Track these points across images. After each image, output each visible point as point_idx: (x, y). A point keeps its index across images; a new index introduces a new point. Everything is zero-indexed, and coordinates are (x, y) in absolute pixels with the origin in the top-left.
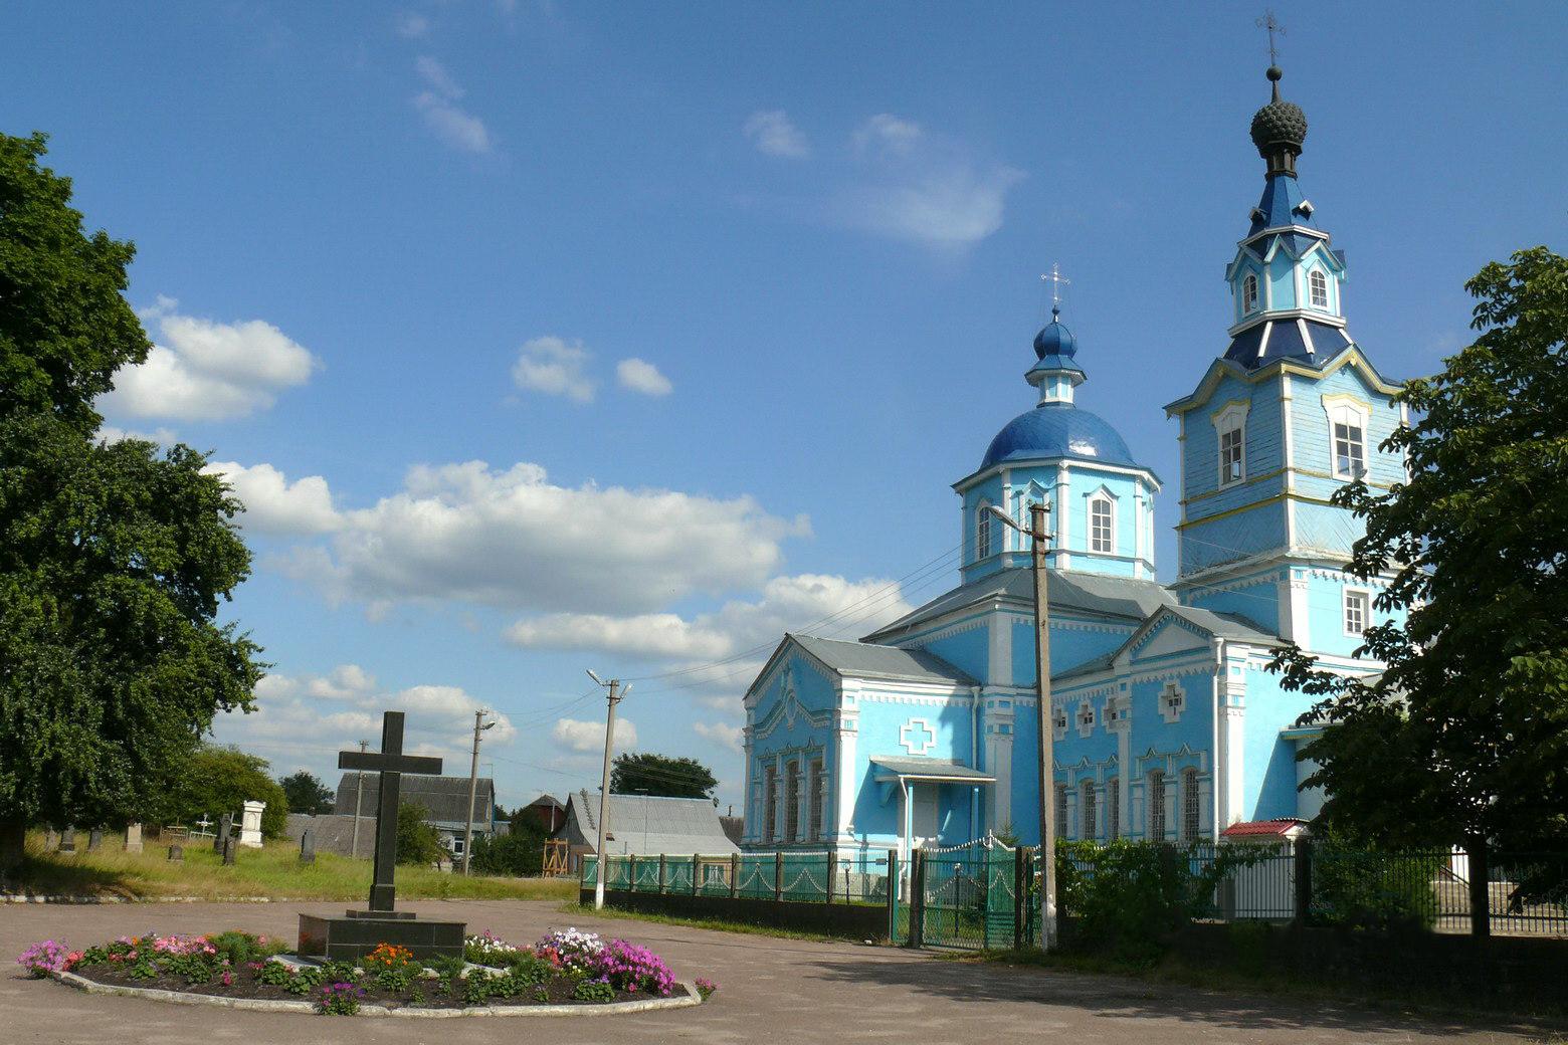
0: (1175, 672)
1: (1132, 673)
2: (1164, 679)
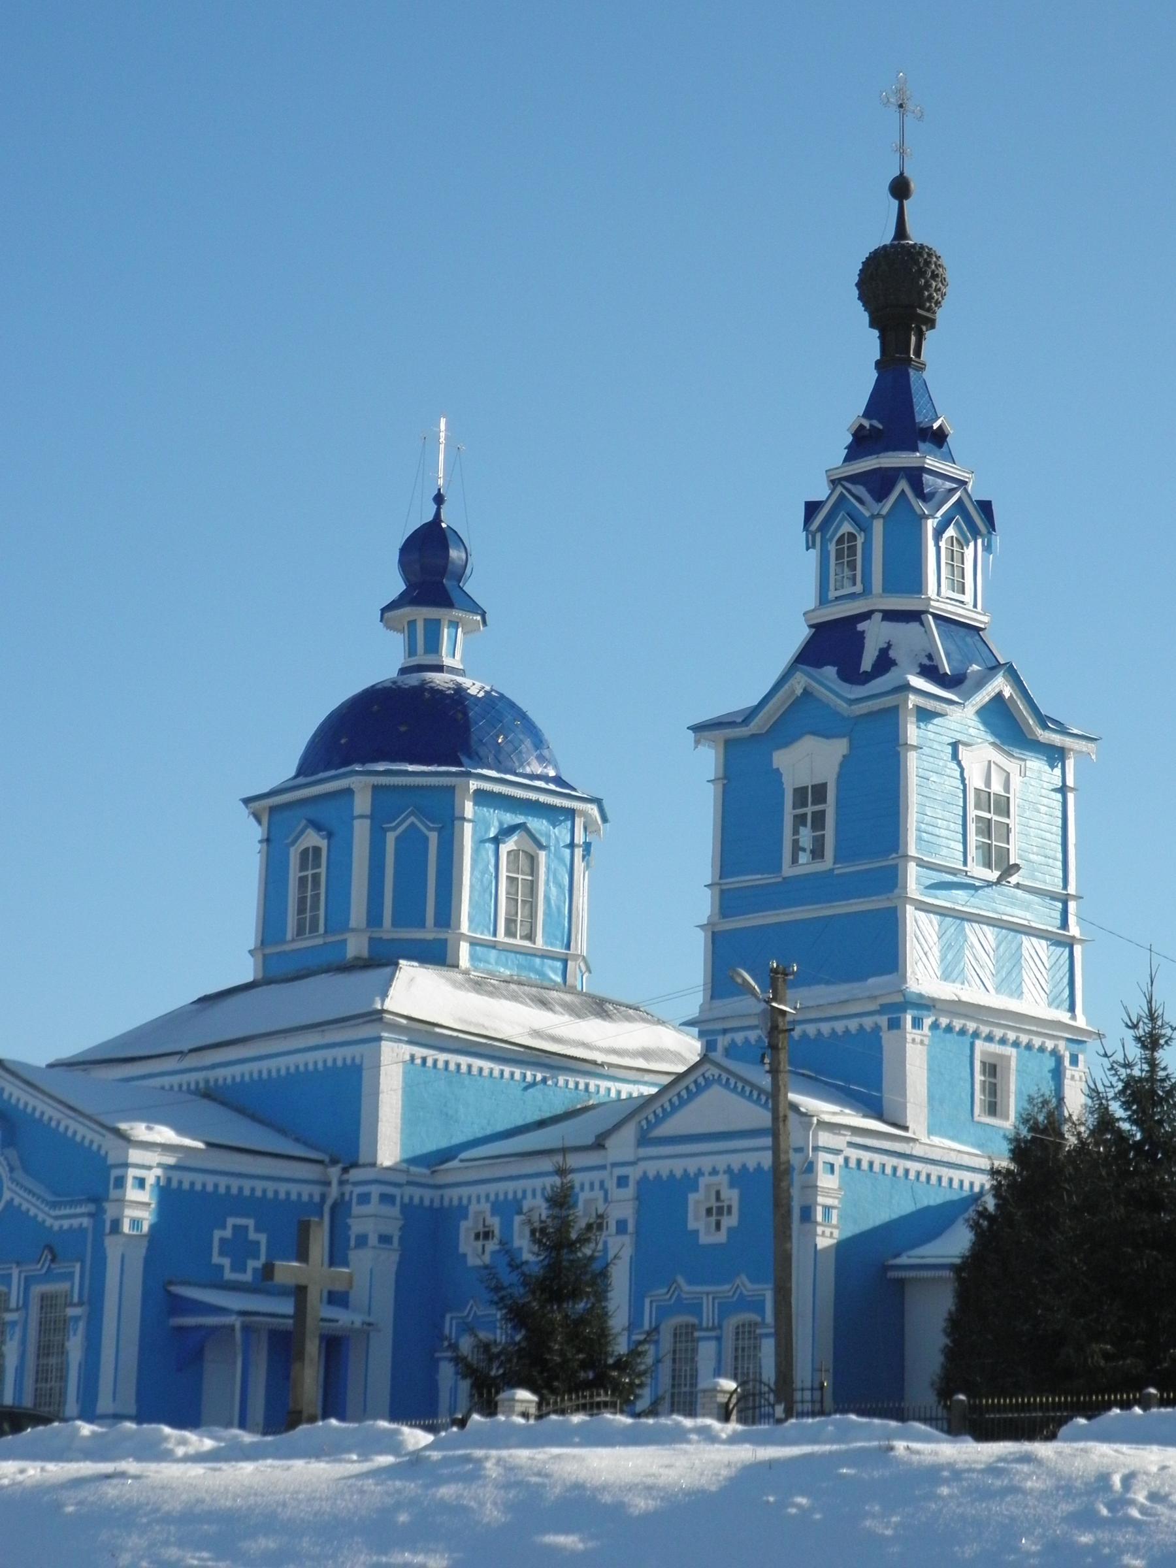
0: (721, 1162)
1: (640, 1159)
2: (700, 1173)
